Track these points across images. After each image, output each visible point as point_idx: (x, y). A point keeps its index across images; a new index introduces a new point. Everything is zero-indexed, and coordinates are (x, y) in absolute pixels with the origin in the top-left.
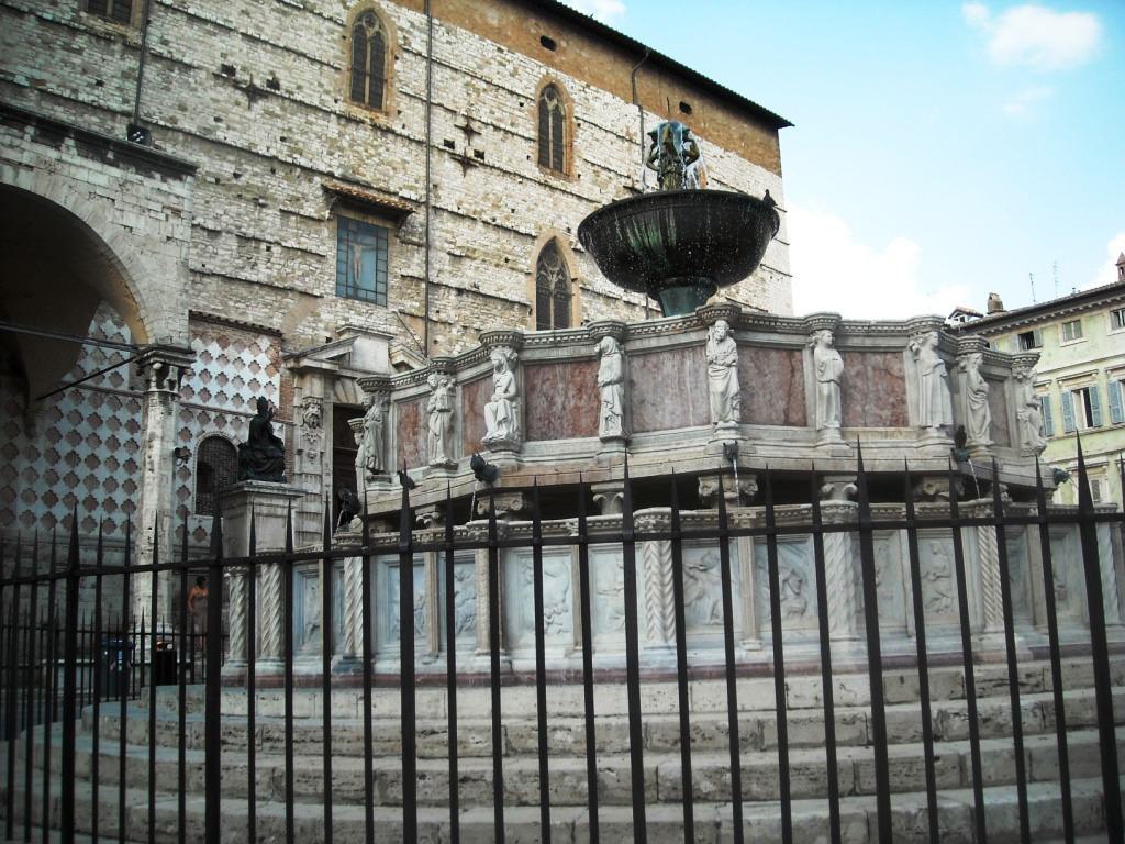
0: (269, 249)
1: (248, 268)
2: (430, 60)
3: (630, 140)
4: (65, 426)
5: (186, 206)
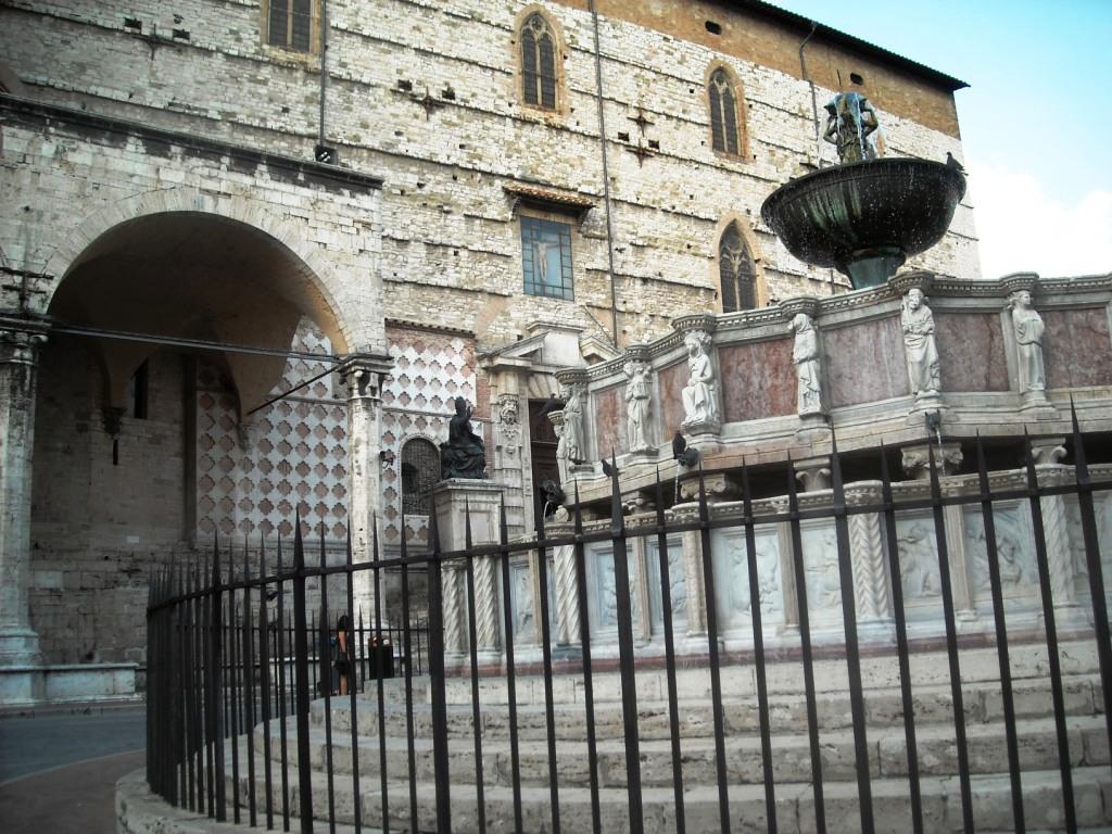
0: (456, 254)
1: (437, 274)
2: (598, 56)
3: (803, 117)
4: (275, 437)
5: (375, 218)
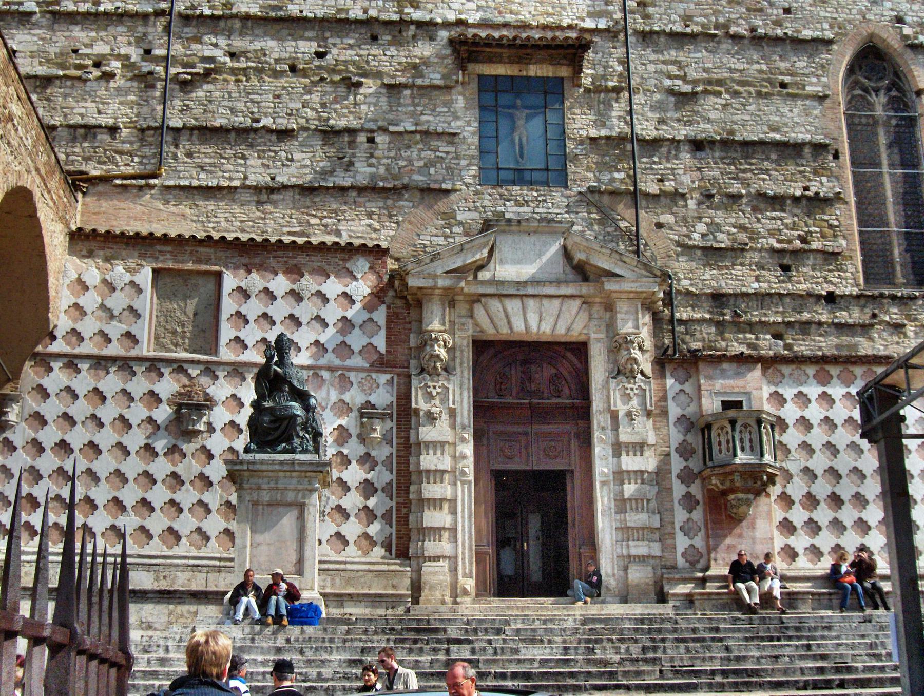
1: (340, 172)
